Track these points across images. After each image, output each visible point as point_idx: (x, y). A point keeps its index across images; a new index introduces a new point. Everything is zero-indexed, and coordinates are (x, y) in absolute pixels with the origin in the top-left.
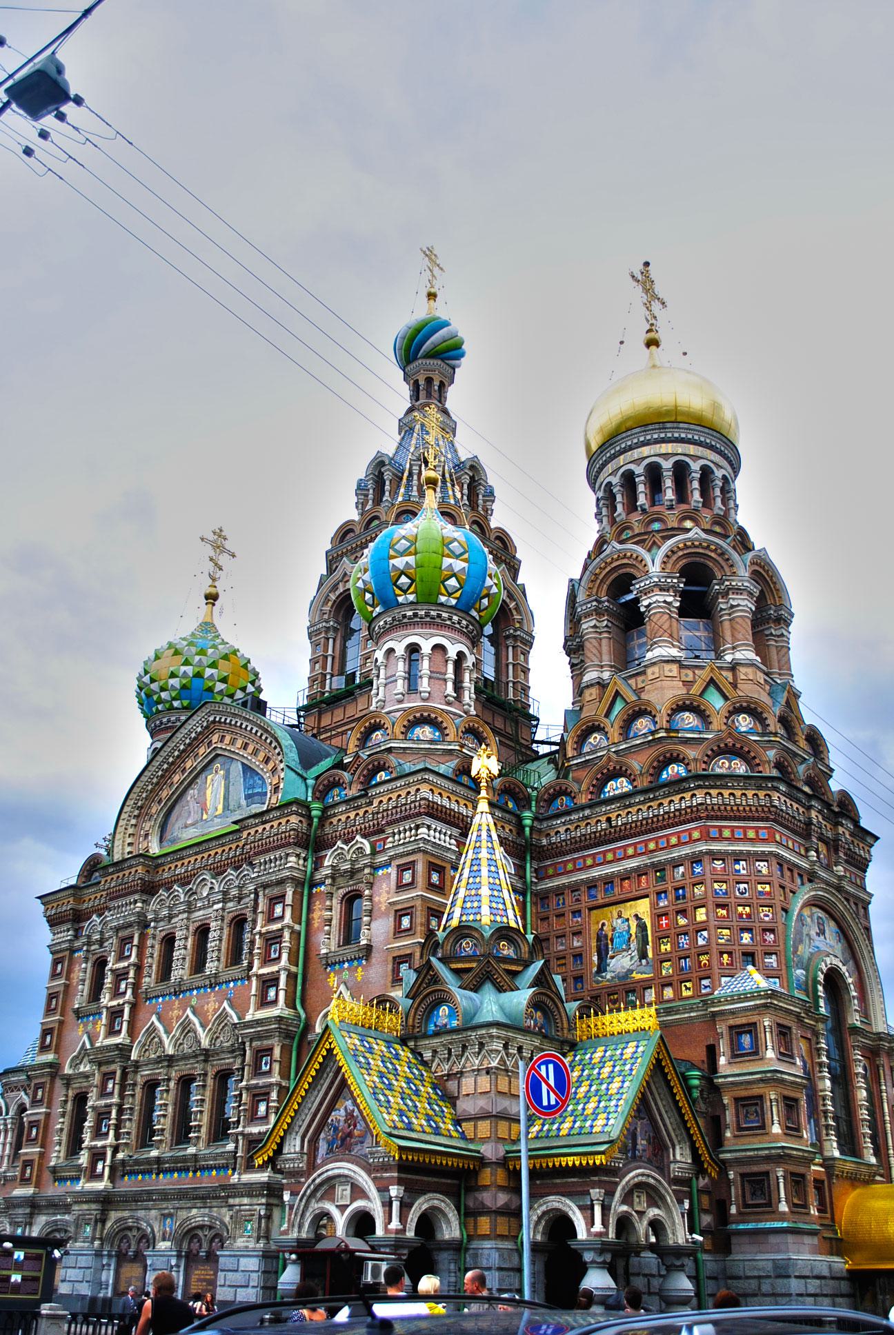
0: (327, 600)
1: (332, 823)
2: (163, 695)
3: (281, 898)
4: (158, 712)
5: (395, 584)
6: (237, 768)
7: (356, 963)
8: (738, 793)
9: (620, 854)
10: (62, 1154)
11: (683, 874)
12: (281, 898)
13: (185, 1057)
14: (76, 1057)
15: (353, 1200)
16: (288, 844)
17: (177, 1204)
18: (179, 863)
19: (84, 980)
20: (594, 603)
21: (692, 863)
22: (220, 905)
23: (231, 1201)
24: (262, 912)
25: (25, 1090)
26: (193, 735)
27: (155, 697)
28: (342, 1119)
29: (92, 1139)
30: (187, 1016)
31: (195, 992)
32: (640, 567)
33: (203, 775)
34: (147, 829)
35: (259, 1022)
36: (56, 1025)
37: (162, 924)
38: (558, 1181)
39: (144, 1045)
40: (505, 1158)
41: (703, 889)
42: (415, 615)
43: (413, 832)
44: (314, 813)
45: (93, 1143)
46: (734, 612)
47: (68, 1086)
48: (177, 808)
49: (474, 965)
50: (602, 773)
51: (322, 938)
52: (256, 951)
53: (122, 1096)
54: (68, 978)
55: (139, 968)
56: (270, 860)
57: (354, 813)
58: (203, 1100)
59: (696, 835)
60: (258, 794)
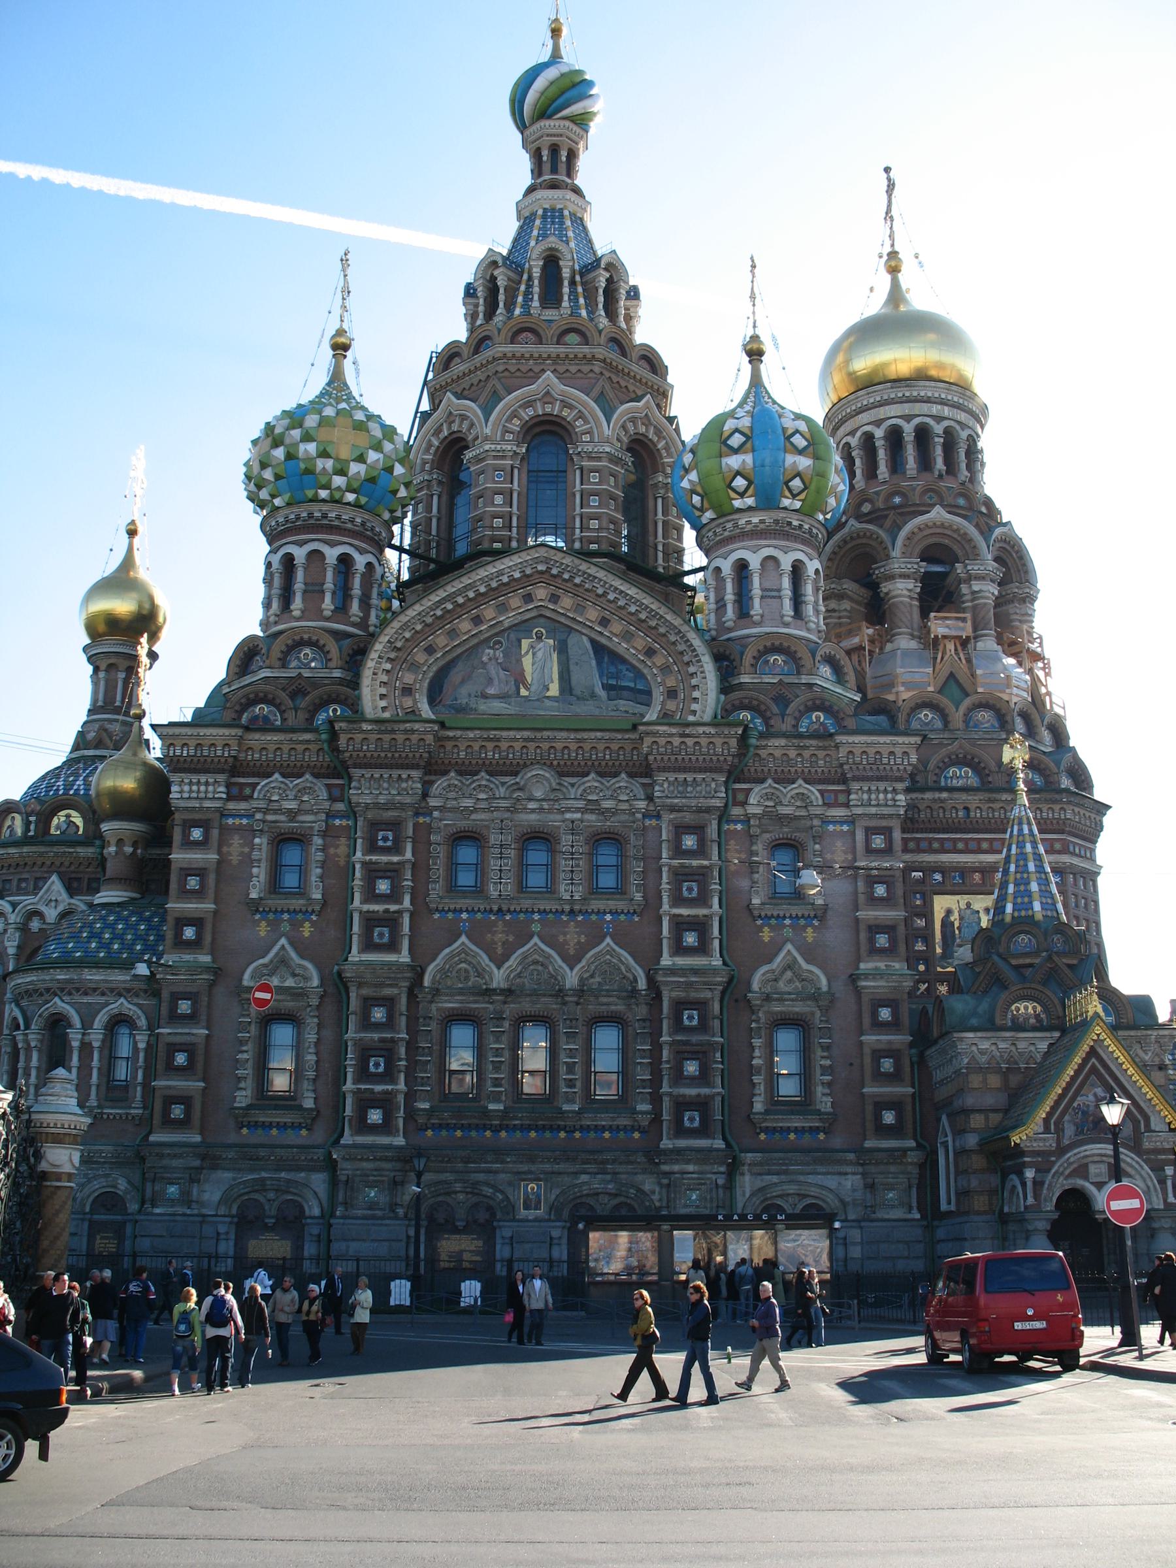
0: (514, 415)
2: (338, 481)
3: (698, 830)
4: (315, 500)
5: (786, 483)
6: (580, 645)
7: (802, 922)
8: (1087, 814)
9: (972, 845)
10: (249, 1093)
12: (698, 830)
13: (534, 993)
17: (547, 1167)
18: (490, 745)
22: (578, 816)
23: (666, 1168)
25: (126, 998)
26: (505, 579)
27: (323, 480)
30: (536, 944)
31: (536, 917)
32: (967, 547)
33: (513, 636)
34: (406, 680)
35: (695, 971)
39: (442, 969)
42: (801, 526)
43: (889, 796)
45: (363, 1087)
48: (460, 666)
49: (1075, 962)
51: (744, 883)
52: (665, 886)
53: (412, 1030)
54: (219, 852)
55: (414, 866)
59: (1058, 846)
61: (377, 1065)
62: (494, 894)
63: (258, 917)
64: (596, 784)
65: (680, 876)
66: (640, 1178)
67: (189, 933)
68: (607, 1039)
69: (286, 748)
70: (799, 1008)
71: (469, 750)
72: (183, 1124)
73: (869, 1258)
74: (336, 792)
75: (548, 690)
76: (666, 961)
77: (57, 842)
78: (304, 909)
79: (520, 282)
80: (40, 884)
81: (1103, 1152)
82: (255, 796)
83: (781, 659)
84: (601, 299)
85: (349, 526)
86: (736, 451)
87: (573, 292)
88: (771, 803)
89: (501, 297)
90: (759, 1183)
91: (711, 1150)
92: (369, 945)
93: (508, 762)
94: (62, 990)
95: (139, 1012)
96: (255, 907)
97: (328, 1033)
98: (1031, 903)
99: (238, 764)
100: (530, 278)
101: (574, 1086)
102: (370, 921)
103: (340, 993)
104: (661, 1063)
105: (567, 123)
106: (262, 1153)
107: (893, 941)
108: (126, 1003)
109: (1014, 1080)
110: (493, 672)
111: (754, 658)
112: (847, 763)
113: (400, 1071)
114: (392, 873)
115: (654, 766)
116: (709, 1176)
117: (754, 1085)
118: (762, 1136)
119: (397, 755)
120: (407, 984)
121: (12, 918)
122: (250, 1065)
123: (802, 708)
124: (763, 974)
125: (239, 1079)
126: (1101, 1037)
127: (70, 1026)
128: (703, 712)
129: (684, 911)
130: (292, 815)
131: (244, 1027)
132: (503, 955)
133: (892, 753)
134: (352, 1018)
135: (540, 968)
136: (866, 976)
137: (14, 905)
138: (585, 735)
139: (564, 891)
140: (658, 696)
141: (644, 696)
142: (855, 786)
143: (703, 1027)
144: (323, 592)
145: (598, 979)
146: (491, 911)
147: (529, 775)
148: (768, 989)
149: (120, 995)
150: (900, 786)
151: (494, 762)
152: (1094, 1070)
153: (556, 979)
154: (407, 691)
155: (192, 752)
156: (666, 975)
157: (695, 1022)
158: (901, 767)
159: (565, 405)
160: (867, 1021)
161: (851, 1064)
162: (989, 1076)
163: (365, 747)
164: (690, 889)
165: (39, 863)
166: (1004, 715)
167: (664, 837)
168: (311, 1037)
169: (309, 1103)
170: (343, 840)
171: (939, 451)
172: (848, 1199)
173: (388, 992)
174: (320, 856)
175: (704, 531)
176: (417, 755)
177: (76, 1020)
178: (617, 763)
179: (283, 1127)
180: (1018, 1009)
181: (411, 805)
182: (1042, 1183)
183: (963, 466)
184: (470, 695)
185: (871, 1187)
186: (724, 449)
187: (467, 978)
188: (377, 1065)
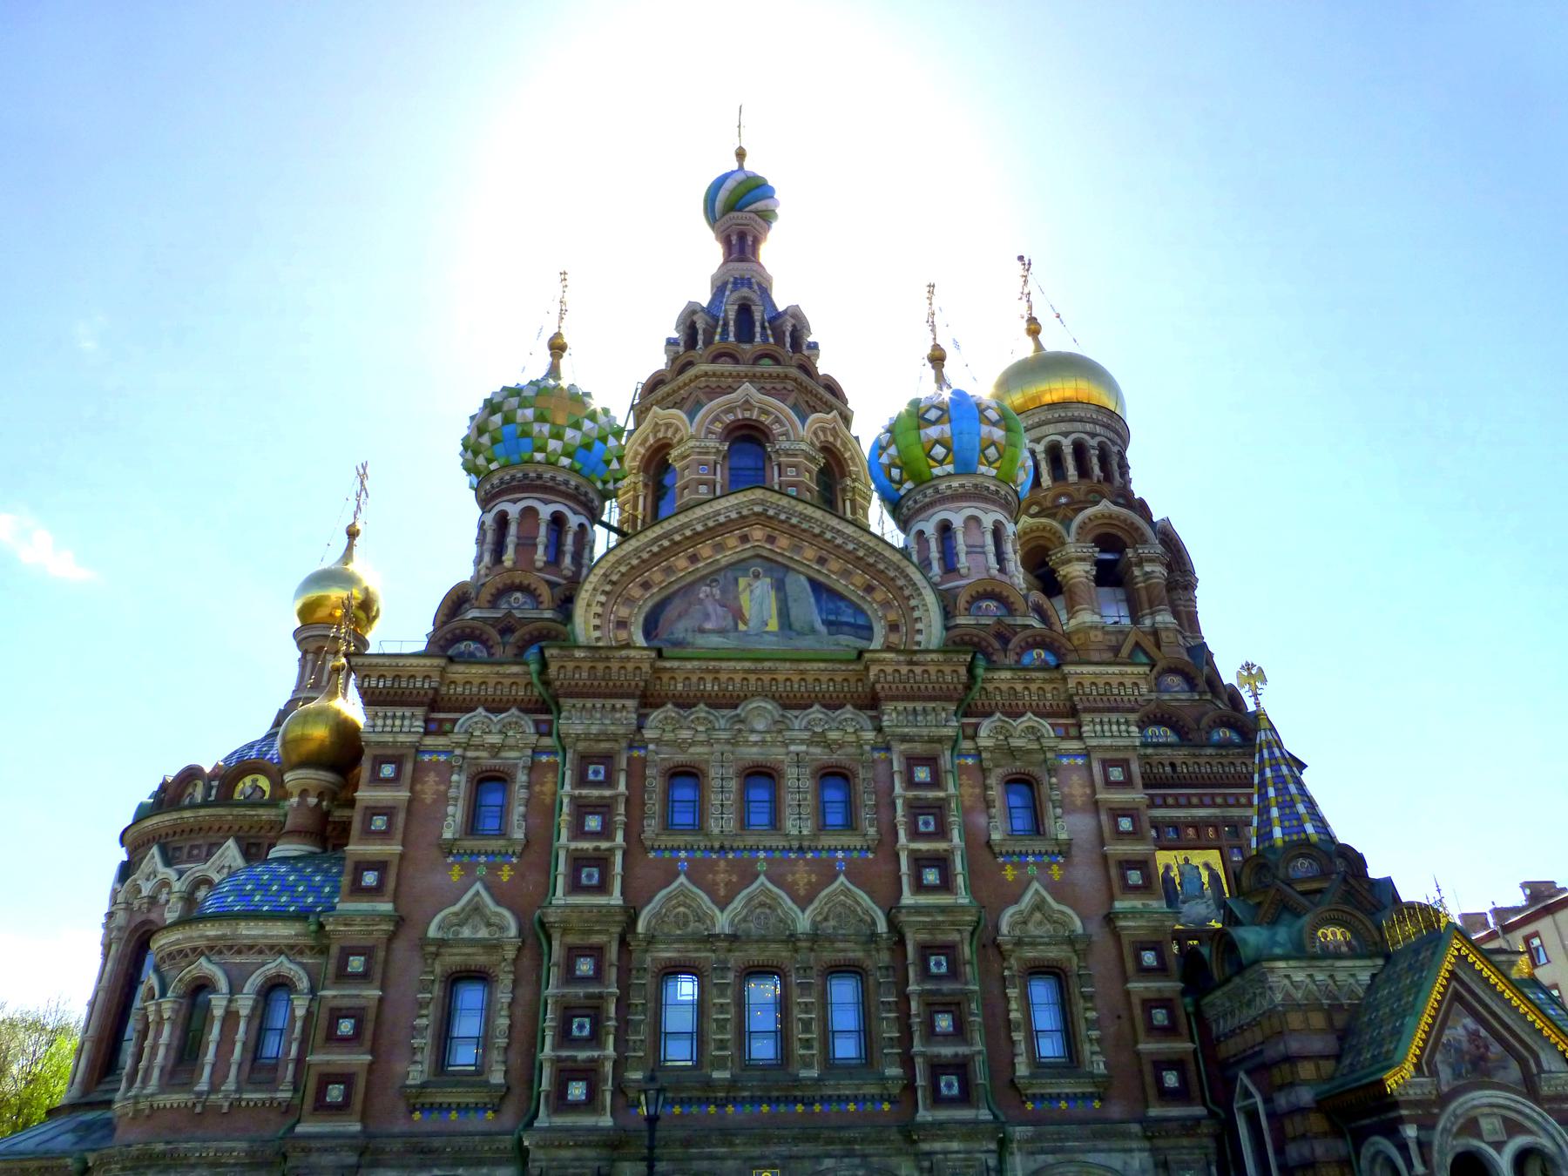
0: (717, 419)
1: (985, 689)
2: (553, 445)
3: (931, 761)
4: (531, 461)
5: (983, 451)
6: (798, 586)
7: (1046, 859)
10: (426, 1067)
12: (931, 761)
13: (763, 939)
14: (456, 914)
16: (948, 699)
17: (783, 1149)
18: (709, 678)
19: (456, 799)
20: (1091, 550)
22: (803, 748)
23: (925, 1147)
24: (901, 772)
25: (287, 956)
26: (722, 519)
27: (539, 443)
28: (1464, 1039)
29: (554, 1048)
30: (762, 884)
31: (762, 855)
32: (1134, 534)
33: (730, 574)
35: (943, 909)
36: (396, 861)
37: (665, 749)
39: (659, 913)
42: (997, 492)
44: (980, 671)
45: (564, 1054)
46: (1189, 606)
47: (437, 955)
50: (1148, 717)
51: (982, 820)
54: (412, 790)
56: (914, 709)
57: (1022, 686)
58: (812, 1003)
60: (848, 624)
61: (581, 1027)
62: (716, 831)
63: (450, 860)
64: (821, 716)
65: (916, 809)
66: (894, 1161)
67: (370, 878)
68: (844, 991)
69: (492, 682)
70: (1053, 953)
71: (687, 682)
72: (342, 1108)
74: (544, 728)
75: (767, 625)
76: (908, 899)
77: (239, 804)
78: (503, 851)
79: (716, 327)
80: (215, 850)
82: (456, 730)
83: (992, 605)
84: (788, 340)
85: (563, 488)
86: (934, 423)
87: (764, 334)
88: (1001, 737)
89: (700, 338)
90: (1033, 1166)
91: (976, 1122)
92: (575, 887)
93: (728, 694)
94: (211, 948)
95: (302, 973)
96: (447, 849)
97: (525, 992)
98: (1301, 825)
99: (439, 699)
100: (726, 324)
101: (810, 1047)
102: (578, 862)
103: (541, 945)
104: (909, 1016)
105: (752, 215)
106: (437, 1143)
108: (286, 962)
109: (1340, 1020)
110: (710, 609)
111: (967, 602)
112: (1077, 694)
113: (608, 1034)
114: (603, 808)
115: (882, 694)
116: (979, 1155)
117: (1013, 1043)
118: (1029, 1106)
119: (611, 684)
120: (619, 929)
121: (177, 886)
122: (429, 1032)
123: (1023, 644)
124: (1011, 916)
125: (414, 1050)
127: (215, 990)
128: (929, 642)
129: (923, 846)
130: (495, 750)
131: (425, 987)
132: (725, 897)
133: (1121, 684)
134: (554, 970)
135: (768, 911)
136: (1125, 914)
137: (181, 874)
138: (808, 666)
139: (790, 825)
140: (879, 630)
141: (866, 631)
142: (1086, 718)
143: (954, 973)
144: (535, 546)
145: (832, 923)
146: (712, 848)
147: (751, 706)
148: (1017, 933)
149: (281, 953)
150: (1133, 717)
151: (713, 694)
152: (1457, 997)
153: (785, 923)
154: (622, 624)
155: (389, 684)
156: (909, 914)
157: (944, 970)
158: (1132, 698)
159: (764, 411)
160: (1130, 965)
161: (1119, 1017)
162: (1310, 1014)
163: (577, 676)
164: (927, 823)
165: (216, 827)
166: (1193, 679)
167: (896, 767)
168: (504, 997)
169: (497, 1077)
170: (550, 777)
171: (1095, 461)
173: (596, 939)
174: (523, 794)
175: (903, 502)
176: (633, 683)
177: (223, 985)
178: (842, 695)
179: (463, 1109)
180: (1325, 936)
181: (625, 736)
183: (1117, 475)
184: (686, 630)
186: (921, 422)
187: (686, 924)
188: (581, 1027)
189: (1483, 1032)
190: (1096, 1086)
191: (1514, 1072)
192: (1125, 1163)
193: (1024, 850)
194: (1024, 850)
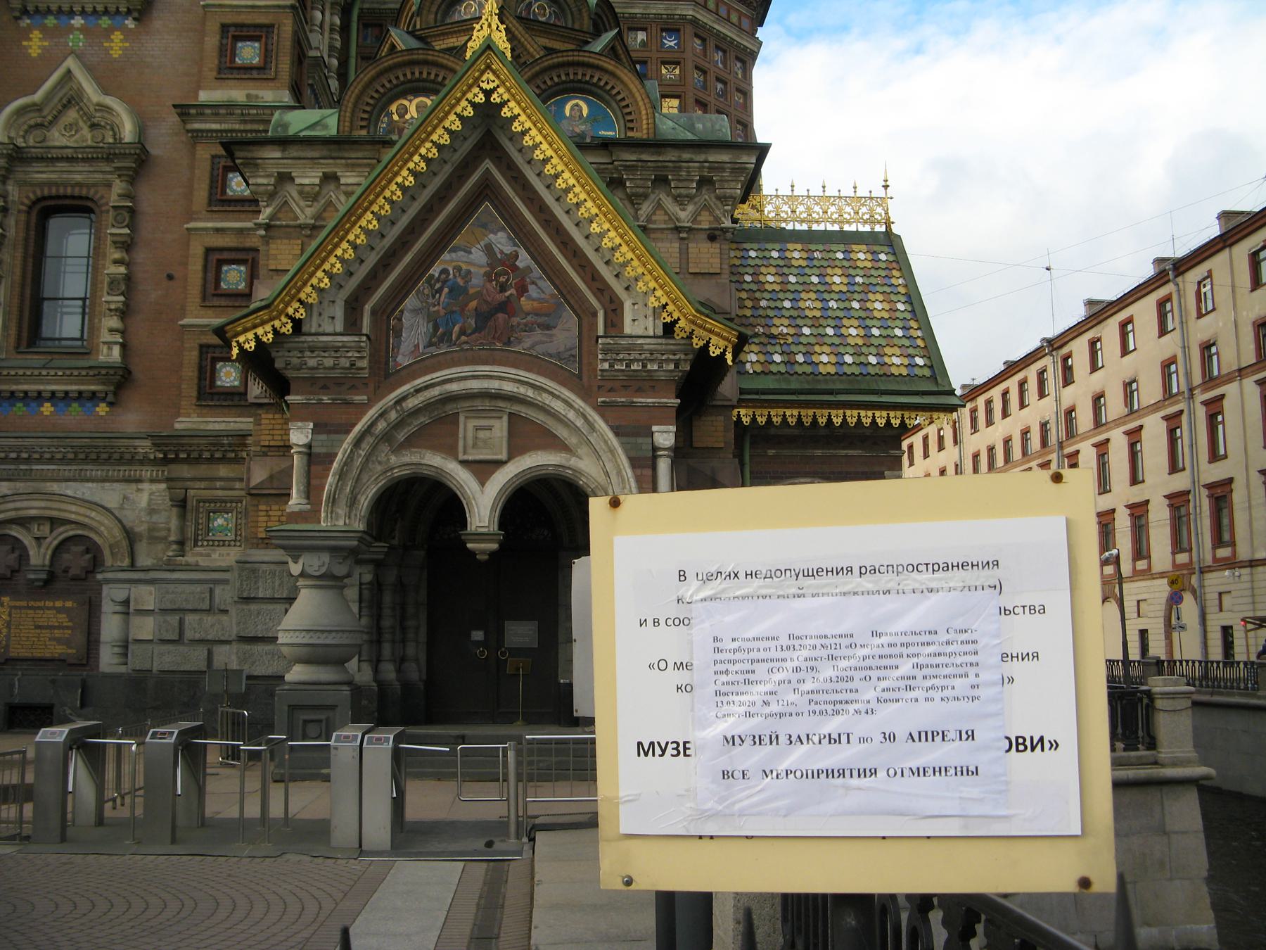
7: (105, 22)
11: (643, 43)
15: (515, 450)
21: (663, 30)
38: (818, 452)
40: (740, 400)
41: (677, 71)
70: (79, 175)
73: (163, 641)
81: (494, 385)
107: (267, 54)
126: (495, 98)
136: (202, 110)
152: (487, 190)
160: (201, 194)
161: (170, 277)
172: (141, 528)
180: (403, 111)
182: (331, 457)
185: (182, 504)
189: (524, 260)
190: (104, 384)
191: (565, 334)
192: (125, 498)
193: (66, 8)
194: (66, 8)
